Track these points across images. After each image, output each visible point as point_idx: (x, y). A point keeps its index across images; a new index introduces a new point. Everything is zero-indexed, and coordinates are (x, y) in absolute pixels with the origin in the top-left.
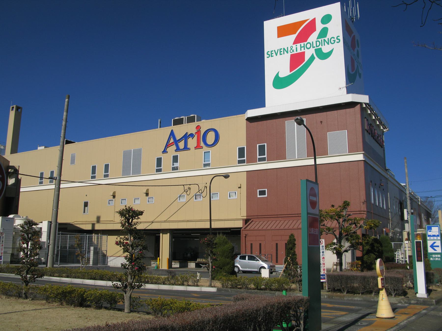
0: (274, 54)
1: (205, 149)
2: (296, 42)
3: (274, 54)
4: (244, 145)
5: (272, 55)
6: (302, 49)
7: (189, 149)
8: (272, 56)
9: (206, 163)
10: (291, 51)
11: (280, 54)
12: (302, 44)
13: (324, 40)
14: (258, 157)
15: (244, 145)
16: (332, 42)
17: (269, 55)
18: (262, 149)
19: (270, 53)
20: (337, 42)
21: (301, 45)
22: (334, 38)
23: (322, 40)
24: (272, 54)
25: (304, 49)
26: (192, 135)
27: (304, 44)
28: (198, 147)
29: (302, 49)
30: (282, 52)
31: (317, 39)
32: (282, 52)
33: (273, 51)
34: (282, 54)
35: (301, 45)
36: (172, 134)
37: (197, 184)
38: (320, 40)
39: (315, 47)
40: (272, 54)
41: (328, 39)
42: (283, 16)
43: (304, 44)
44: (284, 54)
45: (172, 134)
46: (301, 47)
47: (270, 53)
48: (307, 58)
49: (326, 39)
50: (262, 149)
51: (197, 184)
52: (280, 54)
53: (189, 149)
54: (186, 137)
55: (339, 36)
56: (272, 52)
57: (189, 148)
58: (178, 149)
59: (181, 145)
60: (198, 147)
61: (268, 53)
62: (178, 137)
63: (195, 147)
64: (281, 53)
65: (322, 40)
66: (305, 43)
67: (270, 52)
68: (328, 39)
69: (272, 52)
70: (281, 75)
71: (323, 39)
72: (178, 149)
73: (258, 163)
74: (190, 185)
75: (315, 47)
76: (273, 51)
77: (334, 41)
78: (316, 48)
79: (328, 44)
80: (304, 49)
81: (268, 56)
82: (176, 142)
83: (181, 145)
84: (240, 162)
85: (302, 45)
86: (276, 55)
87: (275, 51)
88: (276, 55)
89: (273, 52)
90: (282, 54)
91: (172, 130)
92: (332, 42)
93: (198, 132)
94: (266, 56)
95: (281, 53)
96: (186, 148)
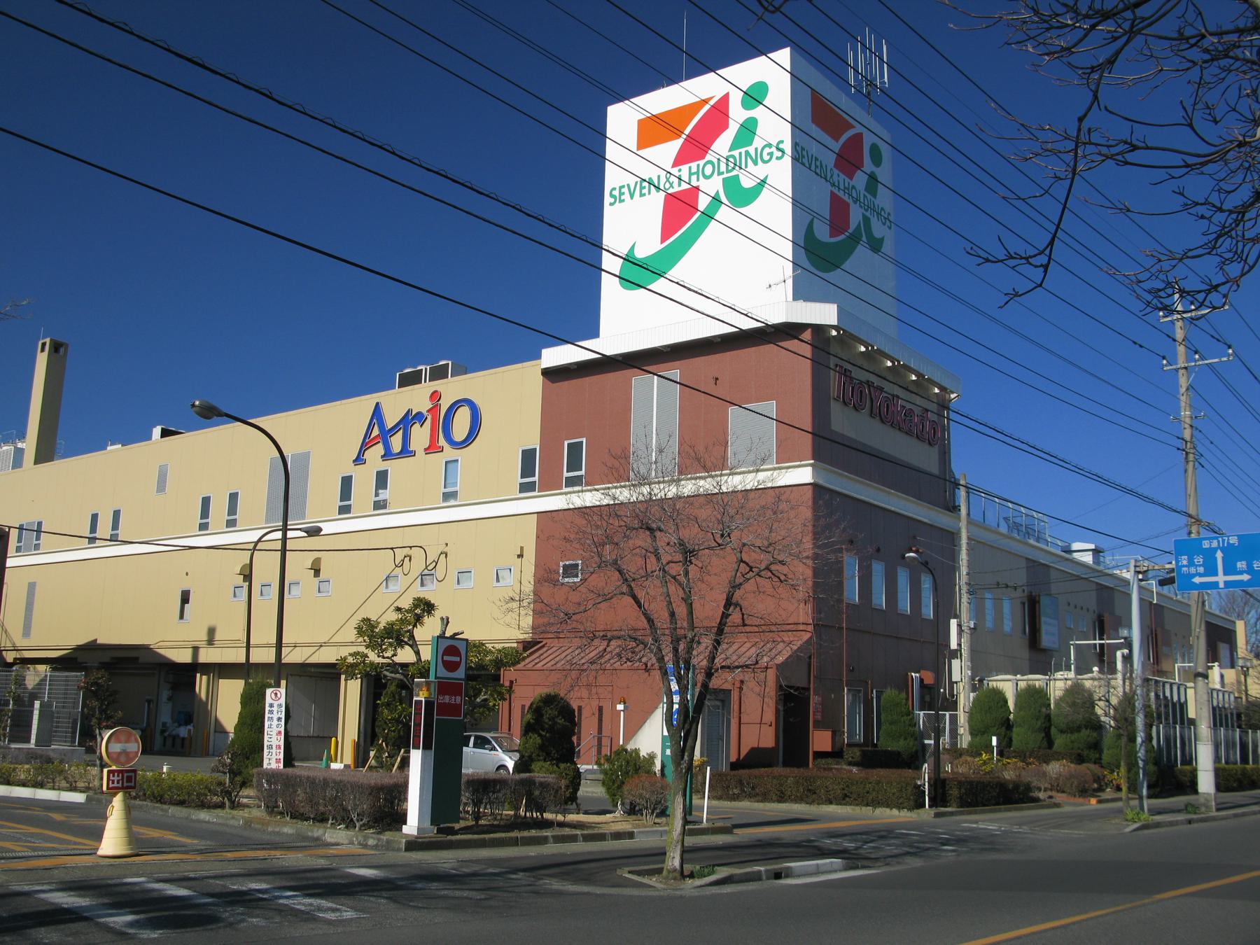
0: (626, 196)
1: (449, 453)
2: (678, 161)
3: (626, 196)
4: (534, 442)
5: (622, 197)
6: (694, 178)
7: (413, 454)
8: (621, 201)
9: (448, 490)
10: (667, 185)
11: (642, 195)
12: (694, 165)
13: (747, 153)
14: (566, 474)
15: (534, 442)
16: (766, 158)
17: (615, 197)
18: (575, 450)
19: (616, 193)
20: (778, 158)
21: (690, 168)
22: (770, 145)
23: (740, 154)
24: (621, 194)
25: (698, 180)
26: (420, 417)
27: (698, 165)
28: (432, 448)
29: (694, 178)
30: (624, 193)
31: (730, 151)
32: (645, 187)
33: (624, 187)
34: (644, 195)
35: (690, 168)
36: (377, 412)
37: (421, 547)
38: (736, 153)
39: (723, 173)
40: (621, 194)
41: (756, 149)
42: (663, 87)
43: (698, 165)
44: (649, 193)
45: (377, 412)
46: (691, 174)
47: (616, 193)
48: (703, 202)
49: (751, 150)
50: (575, 450)
51: (421, 547)
52: (642, 195)
53: (413, 454)
54: (409, 420)
55: (782, 142)
56: (623, 190)
57: (412, 452)
58: (388, 455)
59: (396, 442)
60: (432, 448)
61: (614, 193)
62: (390, 422)
63: (426, 450)
64: (644, 191)
65: (740, 154)
66: (701, 163)
67: (618, 189)
68: (756, 149)
69: (623, 190)
70: (640, 254)
71: (743, 150)
72: (388, 455)
73: (565, 490)
74: (411, 547)
75: (723, 173)
76: (624, 187)
77: (771, 154)
78: (726, 175)
79: (755, 163)
80: (698, 180)
81: (612, 200)
82: (386, 435)
83: (396, 442)
84: (525, 488)
85: (694, 170)
86: (632, 196)
87: (628, 185)
88: (632, 196)
89: (625, 190)
90: (644, 195)
91: (377, 404)
92: (766, 158)
93: (434, 409)
94: (607, 199)
95: (644, 191)
96: (406, 452)
